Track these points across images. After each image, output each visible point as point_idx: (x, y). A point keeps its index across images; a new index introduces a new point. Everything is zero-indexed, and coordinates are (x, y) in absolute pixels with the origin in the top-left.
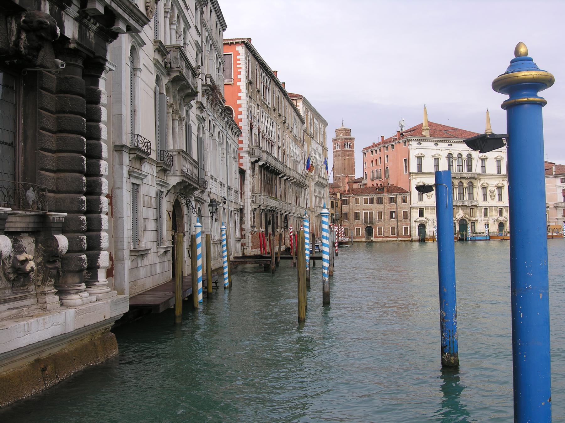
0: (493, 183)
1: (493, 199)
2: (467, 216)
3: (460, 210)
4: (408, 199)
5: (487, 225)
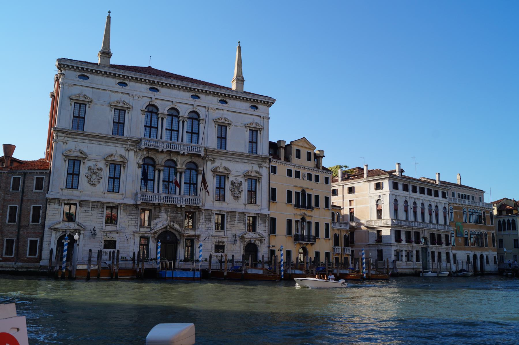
0: (237, 169)
1: (237, 198)
2: (177, 226)
3: (163, 215)
4: (45, 184)
5: (219, 247)
